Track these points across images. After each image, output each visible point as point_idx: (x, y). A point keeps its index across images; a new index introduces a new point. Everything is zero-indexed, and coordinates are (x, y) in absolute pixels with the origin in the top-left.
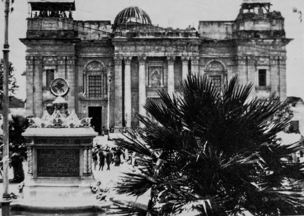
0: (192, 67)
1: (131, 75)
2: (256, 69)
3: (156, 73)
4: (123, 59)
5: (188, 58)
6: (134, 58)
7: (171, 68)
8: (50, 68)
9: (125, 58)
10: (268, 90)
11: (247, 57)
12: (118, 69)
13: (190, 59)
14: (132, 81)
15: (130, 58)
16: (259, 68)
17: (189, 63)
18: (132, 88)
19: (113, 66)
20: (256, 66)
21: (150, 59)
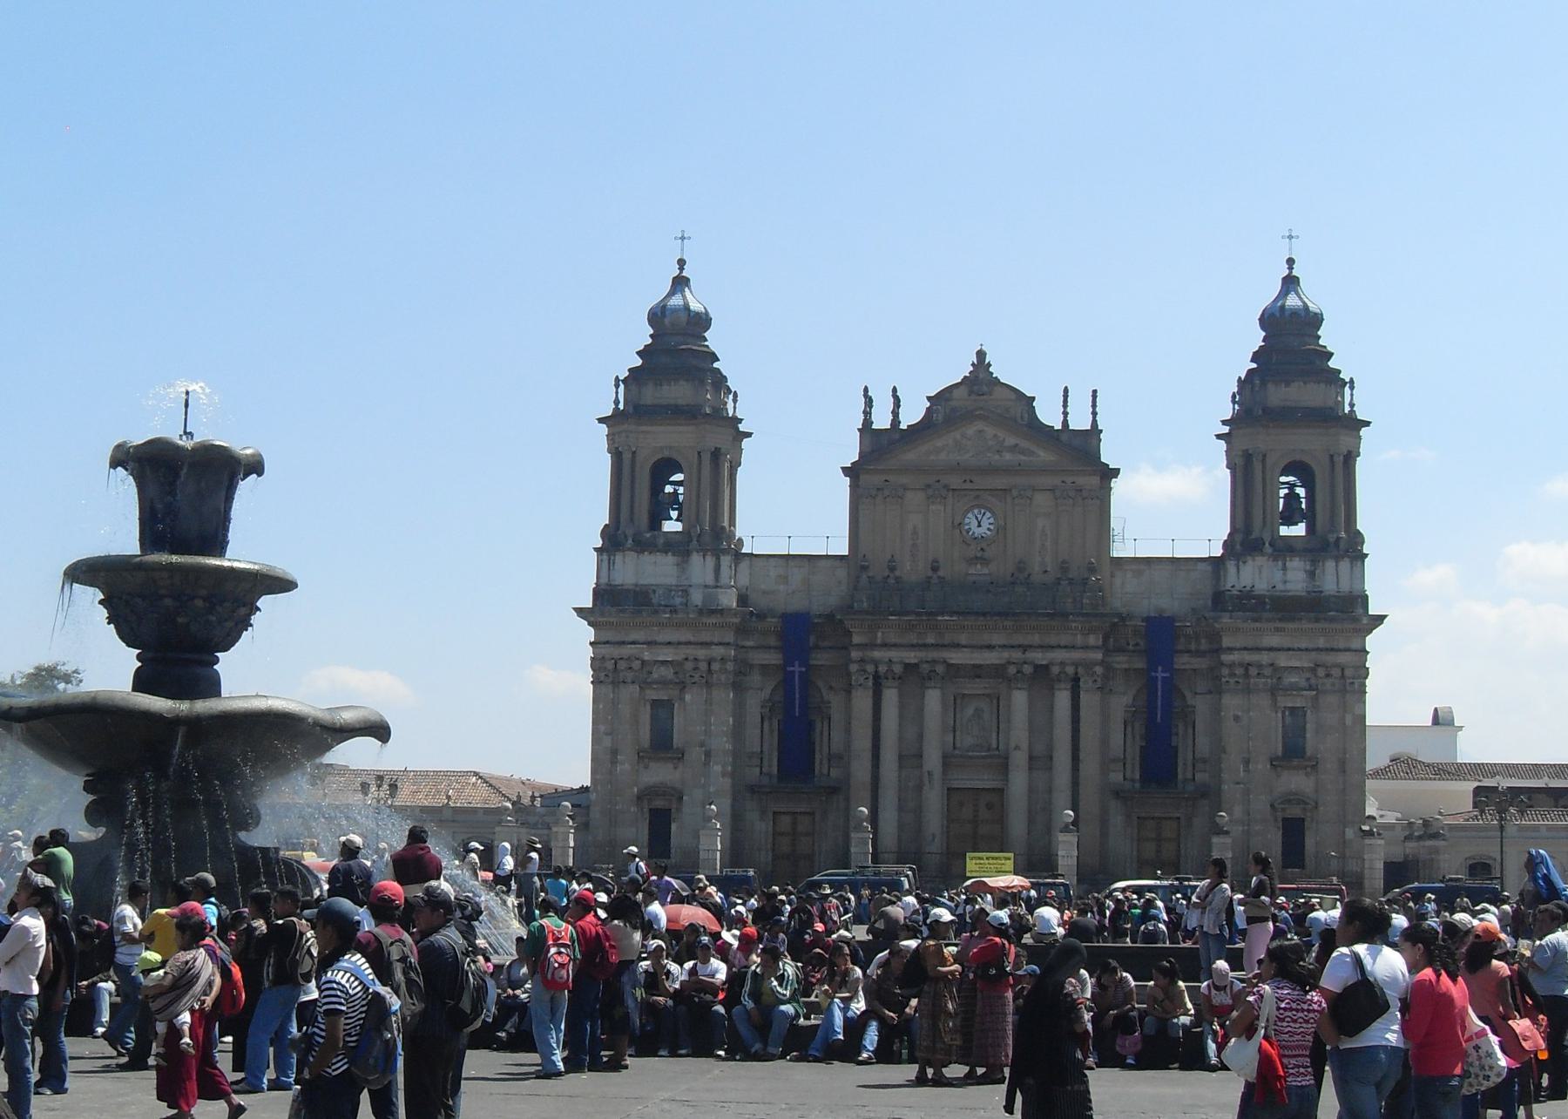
0: (1084, 697)
1: (901, 716)
2: (1275, 702)
3: (978, 713)
4: (876, 672)
5: (1070, 670)
6: (910, 668)
7: (1020, 699)
9: (882, 669)
10: (1309, 769)
11: (1247, 670)
12: (862, 702)
13: (1076, 673)
14: (901, 739)
15: (898, 669)
17: (1073, 687)
18: (901, 757)
19: (848, 691)
20: (1273, 692)
21: (954, 671)
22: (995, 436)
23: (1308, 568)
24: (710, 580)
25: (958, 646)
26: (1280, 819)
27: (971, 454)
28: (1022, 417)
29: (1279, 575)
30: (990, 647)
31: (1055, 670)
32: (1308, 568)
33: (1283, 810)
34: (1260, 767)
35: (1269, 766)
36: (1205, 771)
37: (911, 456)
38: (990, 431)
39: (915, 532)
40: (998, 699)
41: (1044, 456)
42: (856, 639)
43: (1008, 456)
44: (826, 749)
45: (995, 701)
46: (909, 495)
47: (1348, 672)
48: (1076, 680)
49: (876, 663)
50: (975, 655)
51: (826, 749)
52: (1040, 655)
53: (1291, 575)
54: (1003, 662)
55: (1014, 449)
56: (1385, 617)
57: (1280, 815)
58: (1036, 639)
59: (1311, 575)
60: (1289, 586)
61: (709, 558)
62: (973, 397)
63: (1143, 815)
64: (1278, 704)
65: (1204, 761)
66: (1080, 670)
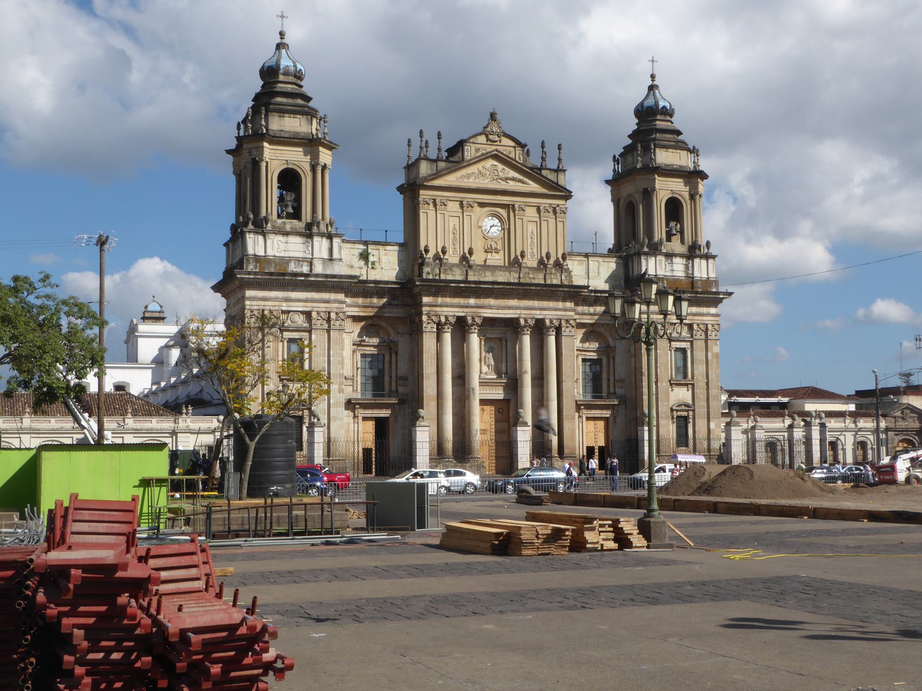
8: (295, 335)
9: (443, 320)
15: (452, 320)
16: (676, 345)
20: (670, 340)
22: (504, 169)
23: (685, 263)
24: (325, 255)
25: (490, 307)
26: (675, 417)
27: (489, 180)
28: (519, 158)
29: (668, 268)
30: (509, 308)
31: (548, 322)
32: (685, 263)
33: (677, 411)
34: (664, 384)
35: (669, 384)
36: (622, 388)
37: (451, 180)
38: (500, 166)
39: (455, 228)
40: (506, 341)
41: (533, 187)
42: (425, 300)
43: (511, 183)
44: (394, 375)
45: (504, 342)
46: (450, 204)
47: (710, 327)
48: (558, 330)
49: (438, 316)
50: (500, 311)
51: (394, 375)
52: (538, 312)
53: (675, 267)
54: (516, 316)
55: (514, 179)
56: (733, 293)
57: (675, 414)
58: (536, 303)
59: (687, 267)
60: (676, 274)
61: (324, 240)
62: (489, 143)
63: (589, 416)
64: (672, 346)
65: (622, 381)
66: (563, 323)
